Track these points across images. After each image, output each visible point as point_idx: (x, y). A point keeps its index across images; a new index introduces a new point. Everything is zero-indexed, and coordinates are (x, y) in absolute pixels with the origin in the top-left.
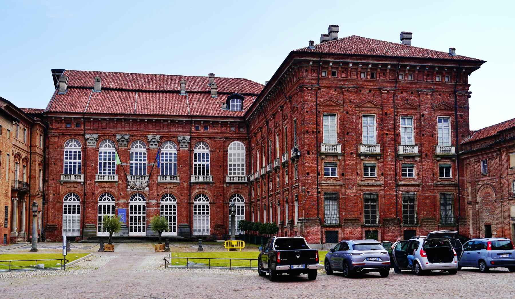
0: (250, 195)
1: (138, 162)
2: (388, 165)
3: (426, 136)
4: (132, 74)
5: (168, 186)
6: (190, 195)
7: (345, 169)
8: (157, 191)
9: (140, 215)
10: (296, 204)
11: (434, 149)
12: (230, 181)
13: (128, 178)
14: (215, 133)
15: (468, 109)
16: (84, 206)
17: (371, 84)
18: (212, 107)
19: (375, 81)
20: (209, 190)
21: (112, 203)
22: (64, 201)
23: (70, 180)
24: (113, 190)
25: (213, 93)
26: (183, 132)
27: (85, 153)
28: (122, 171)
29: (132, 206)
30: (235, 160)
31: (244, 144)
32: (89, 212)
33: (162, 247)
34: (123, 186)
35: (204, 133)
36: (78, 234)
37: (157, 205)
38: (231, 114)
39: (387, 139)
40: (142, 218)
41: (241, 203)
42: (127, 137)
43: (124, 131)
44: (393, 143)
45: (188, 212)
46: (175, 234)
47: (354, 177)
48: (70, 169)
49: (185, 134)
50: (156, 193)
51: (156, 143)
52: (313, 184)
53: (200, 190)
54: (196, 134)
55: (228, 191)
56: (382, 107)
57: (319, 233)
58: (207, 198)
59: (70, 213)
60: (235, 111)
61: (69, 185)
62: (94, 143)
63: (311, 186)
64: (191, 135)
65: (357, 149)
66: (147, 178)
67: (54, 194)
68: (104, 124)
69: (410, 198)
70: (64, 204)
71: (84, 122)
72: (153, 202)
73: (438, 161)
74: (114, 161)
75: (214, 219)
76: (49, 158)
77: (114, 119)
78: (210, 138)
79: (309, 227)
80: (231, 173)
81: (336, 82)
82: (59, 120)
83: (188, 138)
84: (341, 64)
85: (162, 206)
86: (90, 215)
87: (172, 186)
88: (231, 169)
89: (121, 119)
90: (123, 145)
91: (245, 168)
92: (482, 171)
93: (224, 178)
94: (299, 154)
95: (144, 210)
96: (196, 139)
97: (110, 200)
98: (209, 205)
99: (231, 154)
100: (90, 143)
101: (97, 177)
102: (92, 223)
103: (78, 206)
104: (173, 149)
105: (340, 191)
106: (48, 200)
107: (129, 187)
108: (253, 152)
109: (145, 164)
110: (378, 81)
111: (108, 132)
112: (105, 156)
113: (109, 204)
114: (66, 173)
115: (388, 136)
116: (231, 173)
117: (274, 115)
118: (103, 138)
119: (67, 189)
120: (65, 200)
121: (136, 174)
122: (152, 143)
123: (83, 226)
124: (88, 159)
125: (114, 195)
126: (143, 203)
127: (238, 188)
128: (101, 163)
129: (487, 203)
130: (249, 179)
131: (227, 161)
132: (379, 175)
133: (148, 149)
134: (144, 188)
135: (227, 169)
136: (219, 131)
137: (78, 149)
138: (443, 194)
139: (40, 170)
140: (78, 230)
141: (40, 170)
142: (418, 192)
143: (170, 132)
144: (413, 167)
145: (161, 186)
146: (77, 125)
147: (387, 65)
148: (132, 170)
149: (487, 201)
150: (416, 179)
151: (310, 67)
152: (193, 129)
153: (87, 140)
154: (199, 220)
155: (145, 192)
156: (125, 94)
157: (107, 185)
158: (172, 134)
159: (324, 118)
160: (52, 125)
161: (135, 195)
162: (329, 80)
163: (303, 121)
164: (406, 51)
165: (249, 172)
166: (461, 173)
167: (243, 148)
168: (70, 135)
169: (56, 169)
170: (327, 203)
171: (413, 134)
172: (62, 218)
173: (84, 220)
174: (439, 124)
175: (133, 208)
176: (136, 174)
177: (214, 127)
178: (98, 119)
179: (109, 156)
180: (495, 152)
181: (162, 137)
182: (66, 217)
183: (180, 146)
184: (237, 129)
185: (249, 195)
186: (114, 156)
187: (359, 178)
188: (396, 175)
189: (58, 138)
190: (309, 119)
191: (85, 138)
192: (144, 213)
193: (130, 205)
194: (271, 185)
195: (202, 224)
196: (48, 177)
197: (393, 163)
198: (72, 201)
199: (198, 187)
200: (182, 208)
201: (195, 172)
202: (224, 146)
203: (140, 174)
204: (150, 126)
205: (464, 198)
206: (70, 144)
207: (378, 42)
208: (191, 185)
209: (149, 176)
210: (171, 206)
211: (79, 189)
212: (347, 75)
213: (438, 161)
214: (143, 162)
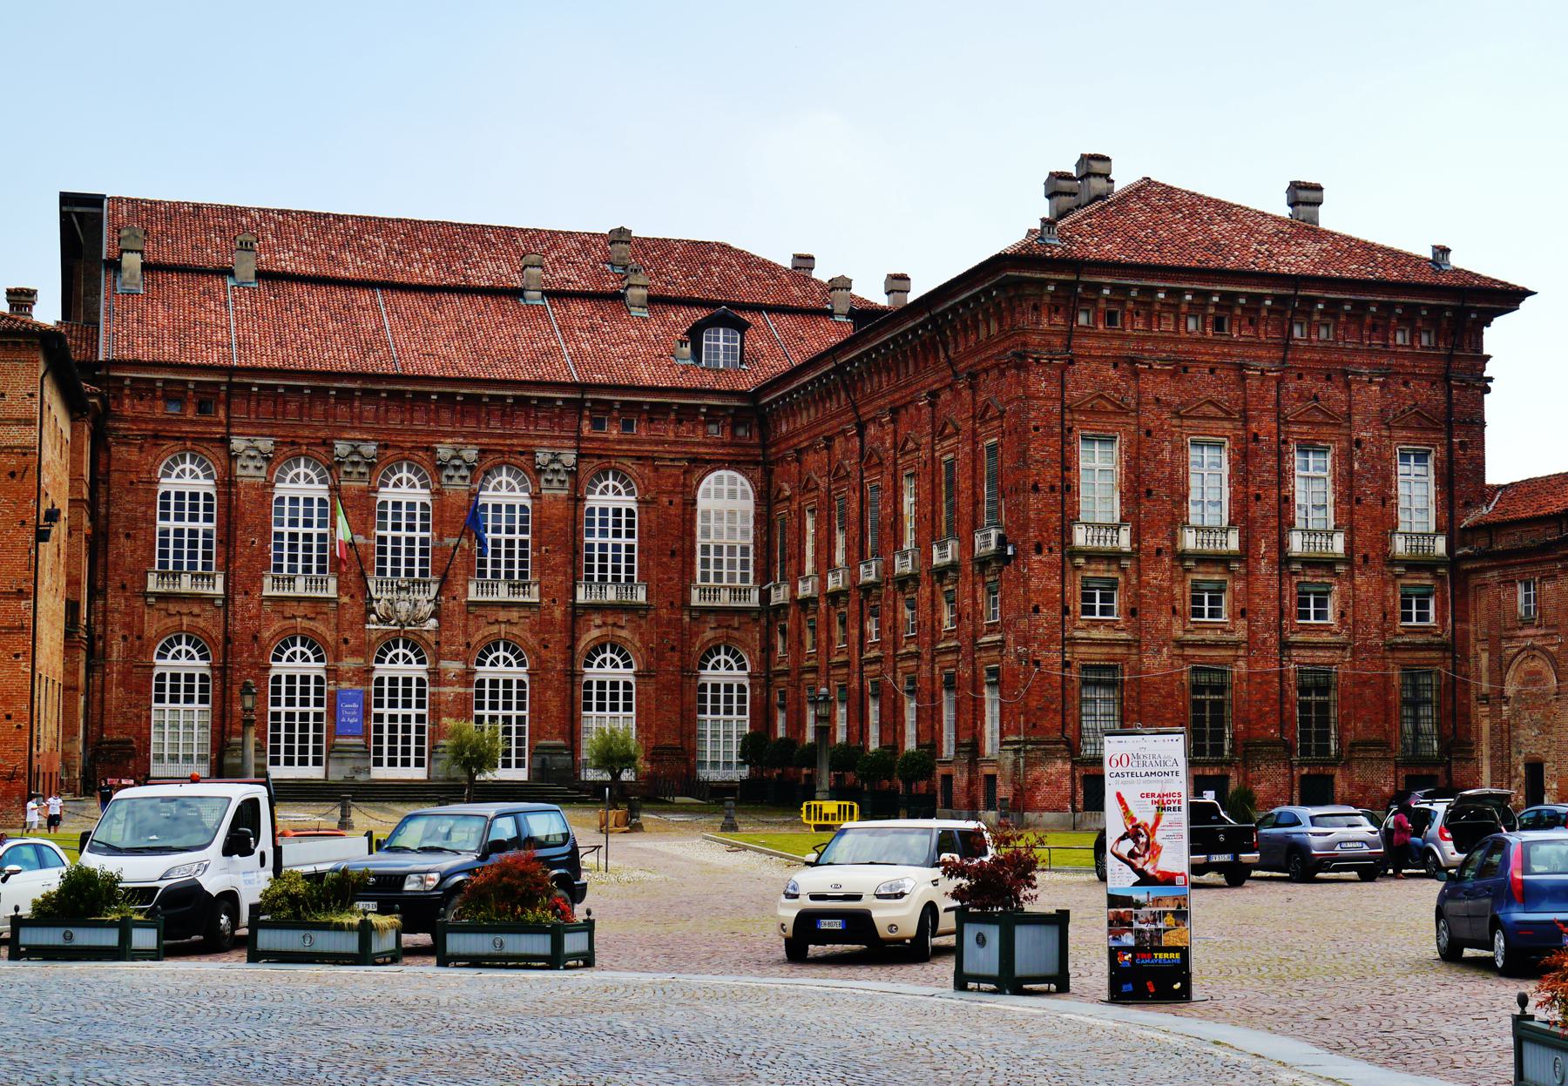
0: (768, 648)
1: (403, 533)
2: (1259, 587)
3: (1363, 501)
4: (340, 218)
5: (502, 615)
6: (572, 647)
7: (1139, 596)
8: (466, 633)
9: (407, 711)
10: (990, 698)
11: (1387, 543)
12: (703, 604)
14: (657, 443)
15: (1483, 425)
16: (224, 677)
17: (1217, 350)
18: (641, 351)
19: (1227, 343)
20: (634, 631)
21: (315, 669)
23: (177, 590)
24: (320, 627)
25: (636, 302)
26: (552, 437)
27: (230, 501)
29: (380, 681)
30: (719, 533)
31: (750, 479)
33: (621, 818)
35: (620, 442)
37: (466, 677)
38: (709, 381)
39: (1257, 511)
40: (413, 719)
41: (738, 676)
42: (370, 449)
43: (360, 429)
44: (1273, 523)
47: (1164, 620)
48: (178, 555)
49: (558, 443)
50: (461, 639)
51: (464, 472)
52: (1051, 640)
53: (604, 630)
54: (595, 445)
55: (697, 634)
56: (1246, 420)
57: (1067, 782)
58: (626, 657)
59: (175, 699)
60: (719, 371)
61: (173, 608)
63: (1044, 645)
64: (578, 448)
65: (1174, 539)
66: (434, 588)
67: (124, 638)
68: (292, 406)
69: (1317, 682)
70: (156, 672)
71: (229, 394)
72: (453, 667)
73: (1399, 576)
76: (108, 515)
77: (328, 389)
78: (639, 458)
79: (1039, 762)
80: (705, 577)
81: (1116, 343)
82: (143, 390)
83: (569, 458)
84: (1134, 294)
85: (481, 683)
87: (514, 615)
88: (705, 563)
89: (354, 390)
90: (355, 476)
91: (751, 558)
92: (1521, 611)
93: (686, 592)
94: (1010, 552)
95: (421, 693)
96: (597, 463)
98: (632, 680)
100: (245, 467)
101: (267, 581)
103: (203, 678)
104: (518, 493)
105: (1125, 660)
106: (105, 655)
107: (373, 617)
108: (782, 511)
109: (424, 541)
110: (1237, 343)
111: (307, 433)
112: (294, 512)
114: (164, 565)
115: (1261, 503)
116: (705, 577)
117: (895, 411)
118: (289, 451)
119: (169, 622)
120: (161, 656)
121: (396, 572)
122: (451, 472)
124: (238, 520)
126: (417, 671)
127: (728, 627)
128: (279, 535)
129: (1528, 701)
130: (765, 596)
131: (693, 535)
132: (1233, 616)
133: (438, 493)
134: (423, 620)
135: (693, 563)
136: (671, 436)
137: (205, 486)
138: (1410, 672)
140: (201, 758)
142: (1341, 665)
143: (512, 436)
144: (1328, 593)
145: (477, 617)
146: (203, 408)
147: (1263, 297)
148: (383, 561)
149: (1532, 694)
150: (1335, 628)
151: (1047, 299)
153: (236, 457)
155: (426, 635)
156: (340, 294)
157: (301, 610)
158: (515, 441)
159: (1083, 448)
160: (121, 404)
162: (1098, 336)
163: (1023, 455)
164: (1311, 248)
166: (1461, 615)
167: (745, 495)
168: (178, 439)
169: (134, 551)
170: (1087, 694)
171: (1331, 499)
172: (149, 718)
173: (223, 726)
174: (1401, 469)
176: (396, 572)
177: (652, 421)
178: (276, 387)
179: (308, 512)
180: (1559, 560)
181: (483, 452)
182: (163, 712)
183: (543, 484)
184: (728, 429)
185: (762, 651)
187: (1177, 624)
188: (1282, 615)
189: (141, 448)
190: (1041, 451)
191: (229, 451)
192: (420, 705)
193: (375, 675)
194: (871, 626)
196: (106, 578)
197: (1274, 582)
198: (183, 661)
199: (598, 621)
200: (546, 688)
201: (590, 568)
202: (684, 485)
203: (410, 573)
204: (445, 415)
205: (1467, 683)
206: (177, 470)
207: (1225, 210)
208: (578, 614)
210: (508, 683)
211: (207, 621)
212: (1149, 324)
213: (1399, 576)
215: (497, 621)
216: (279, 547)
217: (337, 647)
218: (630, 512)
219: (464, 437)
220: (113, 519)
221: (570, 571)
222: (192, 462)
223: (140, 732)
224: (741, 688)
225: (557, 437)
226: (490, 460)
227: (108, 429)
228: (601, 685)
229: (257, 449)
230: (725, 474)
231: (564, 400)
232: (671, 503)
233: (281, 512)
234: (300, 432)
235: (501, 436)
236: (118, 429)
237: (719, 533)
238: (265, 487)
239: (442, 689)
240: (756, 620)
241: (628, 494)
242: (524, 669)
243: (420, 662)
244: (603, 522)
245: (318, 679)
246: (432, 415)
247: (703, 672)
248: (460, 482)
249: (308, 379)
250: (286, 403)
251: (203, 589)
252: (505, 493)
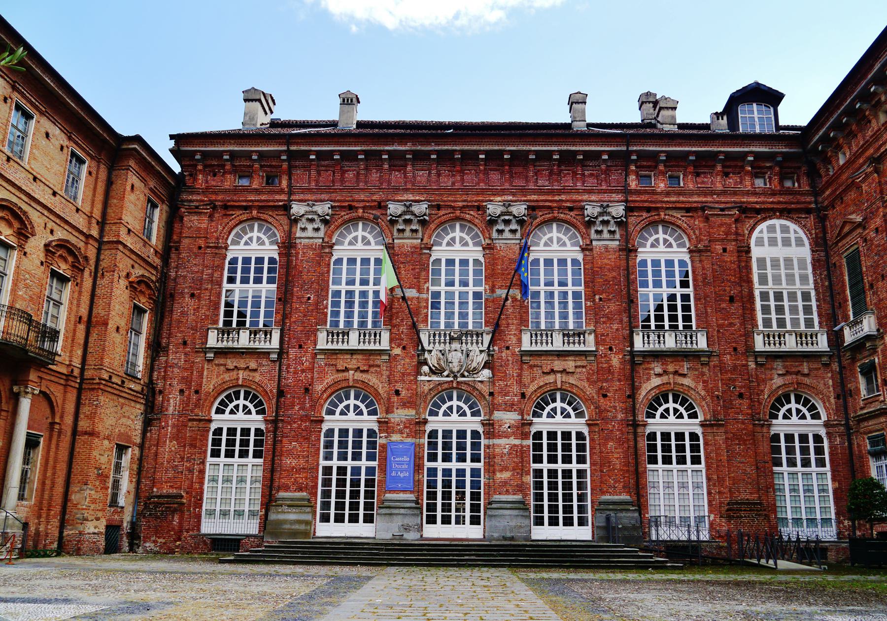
0: (845, 394)
1: (457, 288)
5: (558, 365)
6: (632, 396)
8: (520, 382)
9: (461, 465)
12: (767, 348)
13: (424, 337)
14: (706, 195)
16: (276, 429)
20: (696, 379)
21: (368, 422)
22: (214, 416)
23: (235, 345)
24: (372, 379)
26: (600, 192)
27: (289, 262)
28: (401, 315)
29: (433, 434)
30: (777, 280)
31: (803, 227)
32: (290, 453)
34: (405, 363)
36: (251, 527)
40: (468, 473)
41: (813, 427)
42: (421, 209)
45: (633, 457)
46: (582, 533)
49: (606, 197)
50: (515, 389)
51: (514, 226)
53: (665, 379)
54: (644, 197)
55: (764, 381)
58: (691, 407)
61: (231, 363)
62: (317, 230)
64: (626, 201)
66: (487, 339)
68: (350, 175)
70: (213, 426)
71: (290, 167)
72: (507, 418)
74: (376, 288)
75: (721, 480)
77: (381, 152)
78: (688, 210)
80: (767, 323)
83: (618, 210)
85: (538, 435)
86: (294, 462)
87: (570, 364)
88: (766, 309)
90: (408, 234)
91: (814, 303)
93: (749, 336)
95: (475, 446)
96: (647, 213)
97: (361, 413)
98: (699, 431)
99: (762, 262)
100: (304, 229)
101: (322, 336)
102: (300, 489)
106: (162, 409)
107: (425, 369)
111: (362, 197)
113: (358, 426)
116: (767, 323)
119: (227, 376)
120: (219, 411)
123: (269, 501)
124: (298, 279)
125: (377, 394)
126: (472, 424)
127: (798, 373)
128: (337, 294)
130: (835, 338)
131: (750, 282)
133: (489, 248)
134: (474, 371)
135: (753, 310)
136: (719, 187)
139: (139, 311)
140: (252, 514)
141: (139, 311)
143: (559, 192)
145: (532, 367)
152: (633, 183)
153: (296, 221)
154: (668, 485)
155: (479, 386)
157: (353, 362)
158: (563, 197)
161: (443, 393)
165: (832, 316)
167: (799, 242)
168: (245, 208)
169: (197, 310)
172: (202, 472)
173: (272, 480)
175: (440, 440)
176: (449, 325)
177: (698, 175)
178: (332, 152)
181: (532, 208)
182: (216, 467)
183: (593, 236)
185: (838, 397)
186: (378, 272)
189: (211, 216)
191: (289, 216)
193: (429, 428)
195: (680, 500)
196: (170, 335)
198: (240, 415)
199: (658, 370)
200: (607, 439)
202: (737, 234)
204: (495, 176)
206: (246, 238)
208: (636, 362)
209: (494, 333)
210: (566, 435)
211: (264, 377)
214: (471, 289)
215: (552, 371)
216: (336, 304)
218: (682, 263)
219: (514, 195)
220: (181, 280)
221: (625, 319)
222: (259, 231)
223: (191, 486)
224: (818, 438)
225: (605, 191)
226: (541, 216)
227: (183, 201)
228: (666, 436)
229: (315, 213)
230: (777, 222)
231: (609, 153)
232: (725, 250)
233: (338, 272)
234: (356, 197)
235: (551, 192)
236: (191, 201)
237: (777, 280)
238: (323, 247)
239: (496, 441)
240: (826, 365)
241: (679, 246)
242: (583, 421)
243: (475, 414)
244: (657, 273)
245: (371, 433)
246: (481, 175)
247: (774, 421)
248: (509, 236)
249: (363, 144)
250: (343, 172)
251: (261, 344)
252: (555, 246)
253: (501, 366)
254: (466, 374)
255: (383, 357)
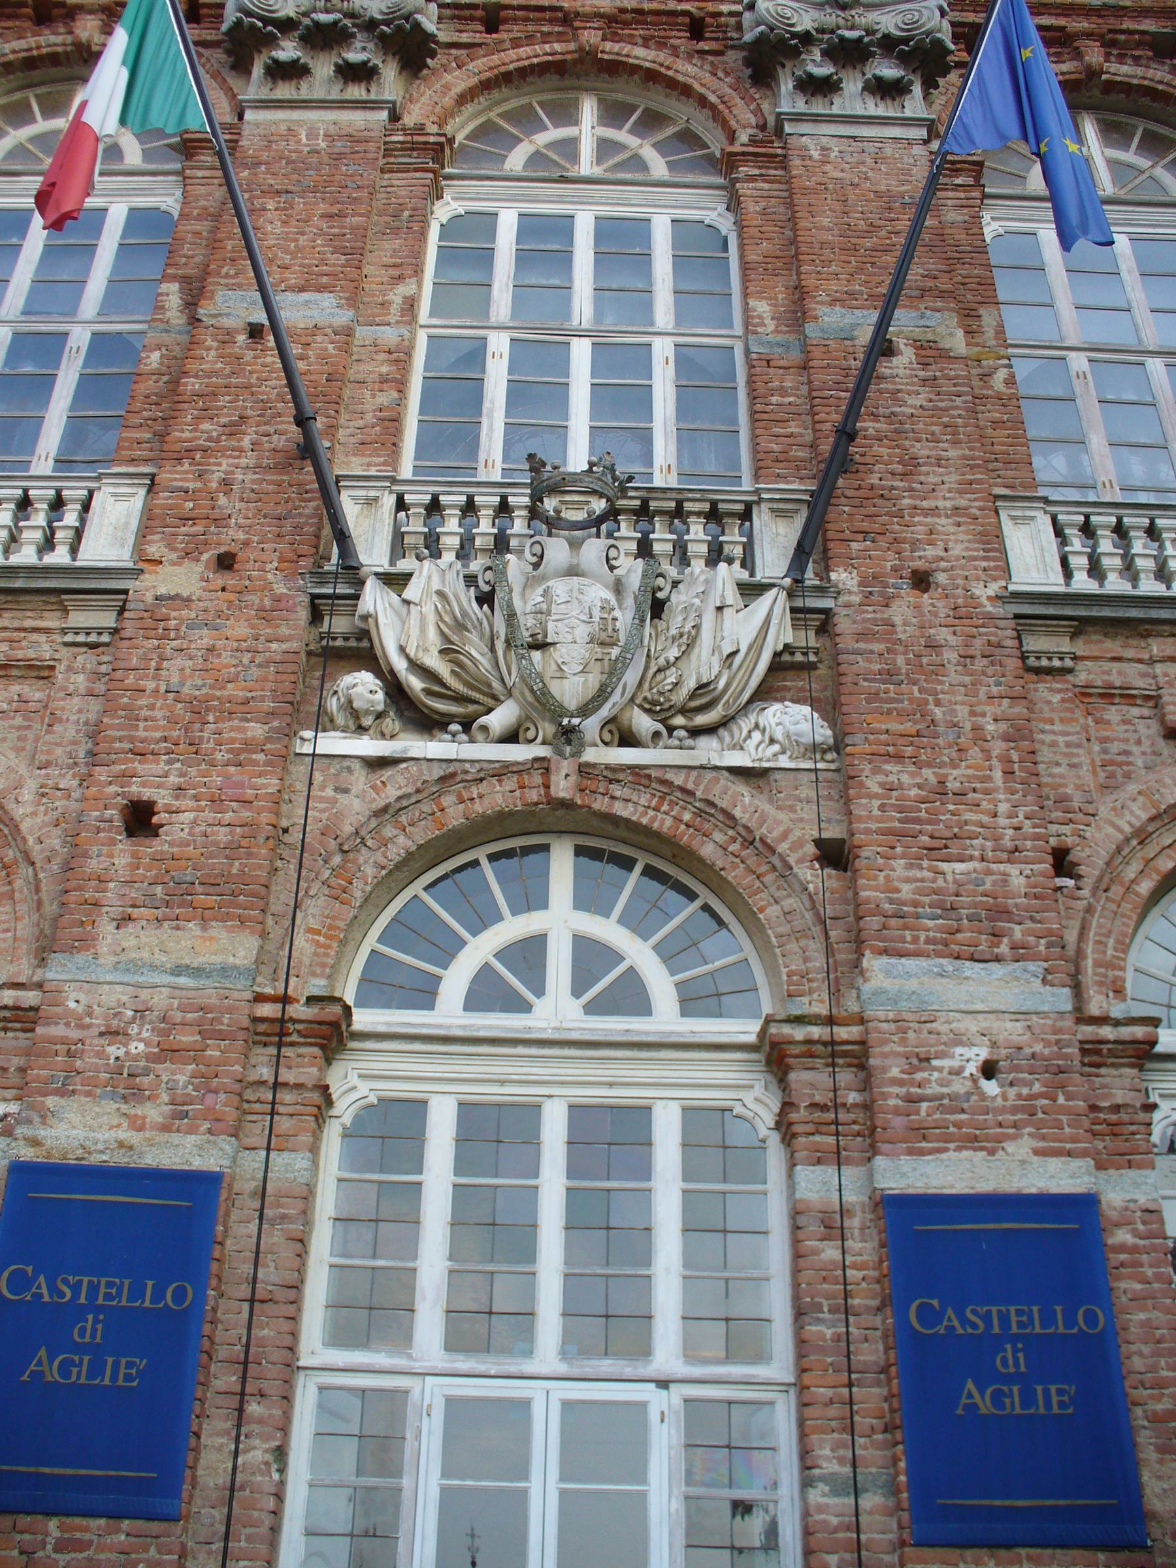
8: (1025, 770)
66: (775, 542)
193: (354, 1084)
209: (818, 507)
217: (75, 854)
253: (889, 675)
254: (644, 723)
255: (78, 619)
